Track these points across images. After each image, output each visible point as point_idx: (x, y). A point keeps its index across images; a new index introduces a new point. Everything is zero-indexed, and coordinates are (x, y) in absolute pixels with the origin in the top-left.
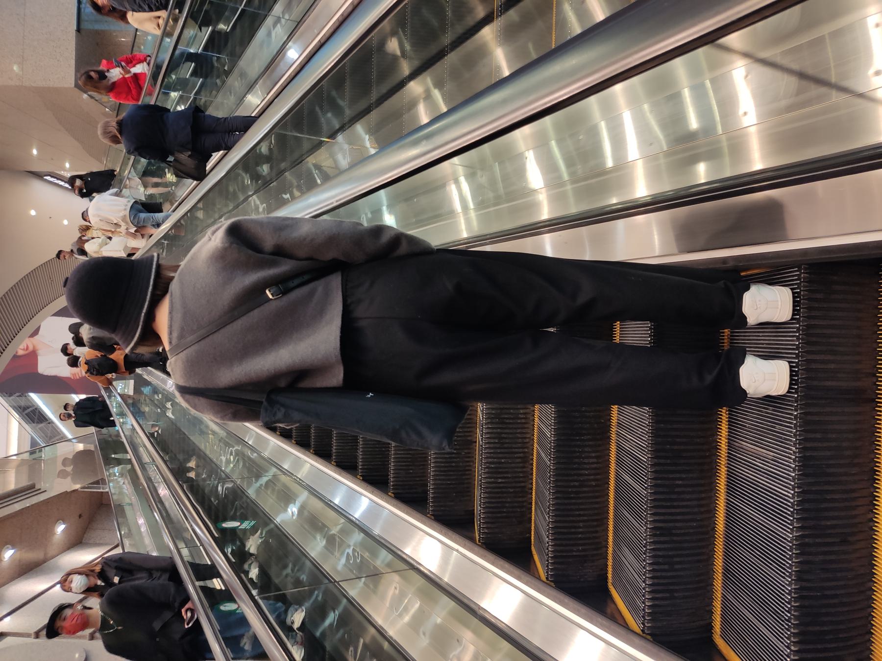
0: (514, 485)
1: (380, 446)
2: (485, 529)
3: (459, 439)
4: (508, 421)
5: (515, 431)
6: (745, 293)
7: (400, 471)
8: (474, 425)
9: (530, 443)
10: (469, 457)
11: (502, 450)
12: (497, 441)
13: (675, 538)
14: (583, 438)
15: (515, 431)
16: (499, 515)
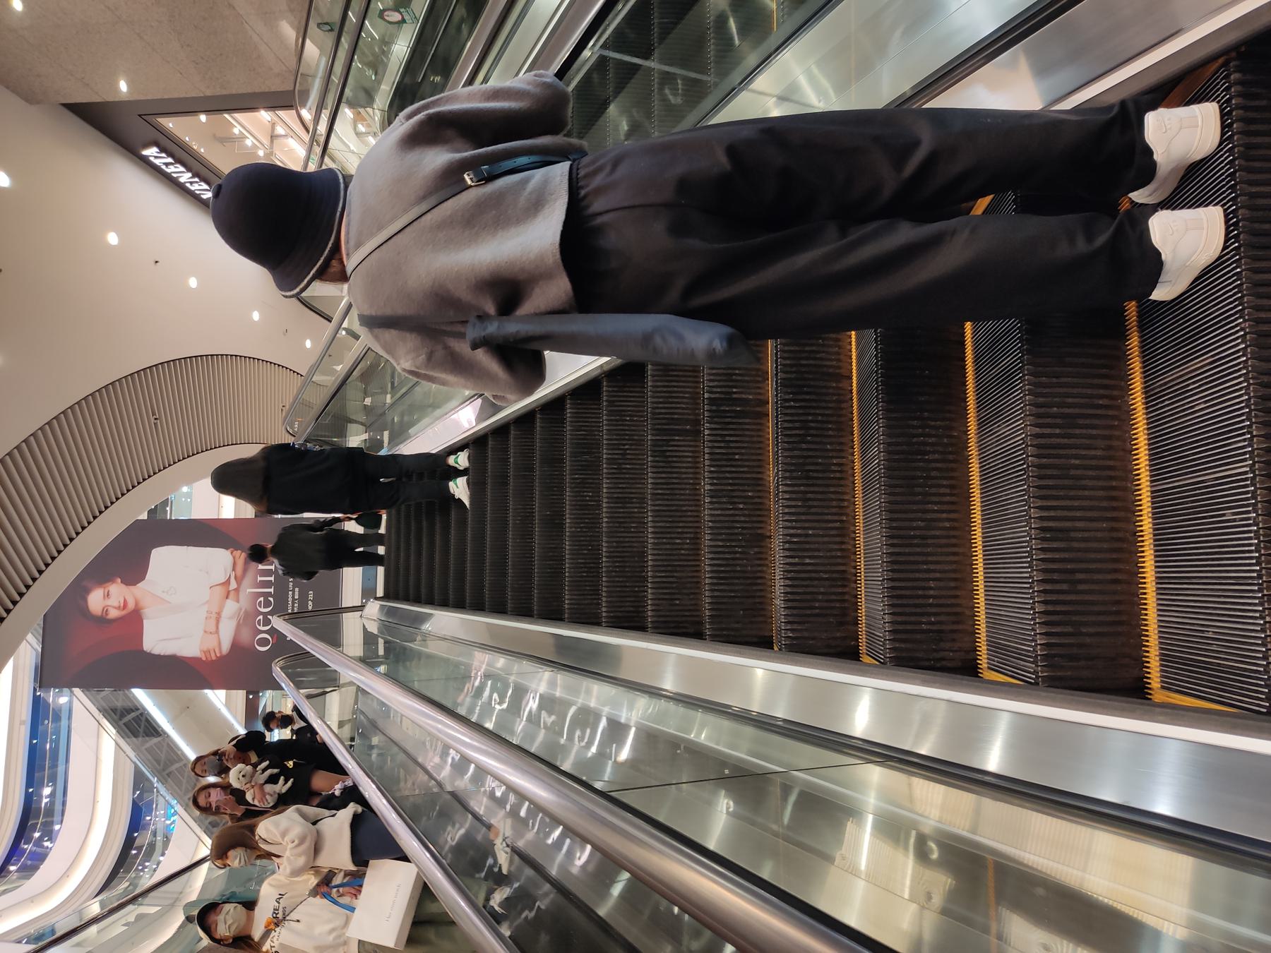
0: (828, 568)
1: (631, 585)
2: (789, 632)
3: (745, 532)
4: (815, 475)
5: (825, 489)
6: (1147, 114)
7: (661, 602)
8: (766, 513)
9: (851, 508)
10: (760, 559)
11: (809, 517)
12: (800, 504)
13: (1075, 545)
14: (927, 457)
15: (825, 489)
16: (809, 612)
